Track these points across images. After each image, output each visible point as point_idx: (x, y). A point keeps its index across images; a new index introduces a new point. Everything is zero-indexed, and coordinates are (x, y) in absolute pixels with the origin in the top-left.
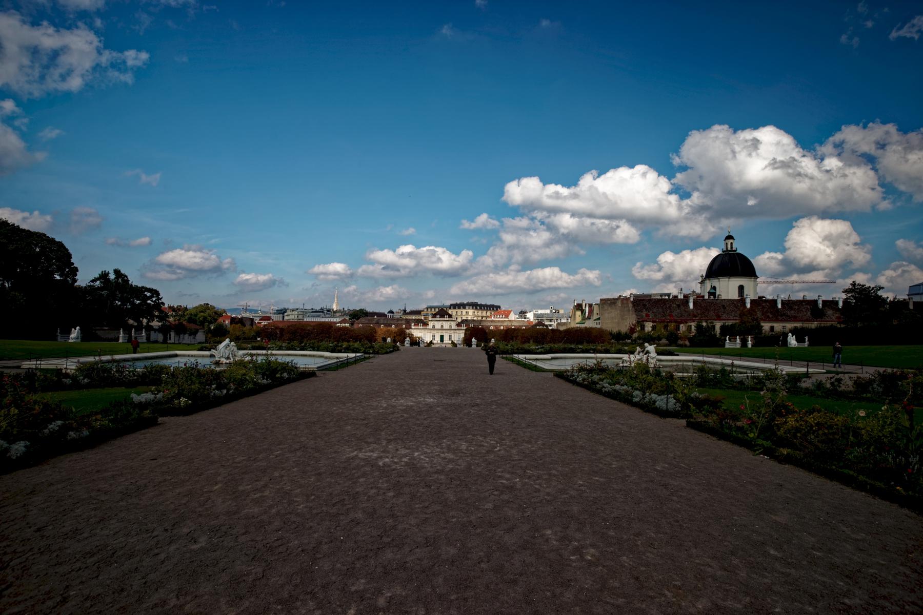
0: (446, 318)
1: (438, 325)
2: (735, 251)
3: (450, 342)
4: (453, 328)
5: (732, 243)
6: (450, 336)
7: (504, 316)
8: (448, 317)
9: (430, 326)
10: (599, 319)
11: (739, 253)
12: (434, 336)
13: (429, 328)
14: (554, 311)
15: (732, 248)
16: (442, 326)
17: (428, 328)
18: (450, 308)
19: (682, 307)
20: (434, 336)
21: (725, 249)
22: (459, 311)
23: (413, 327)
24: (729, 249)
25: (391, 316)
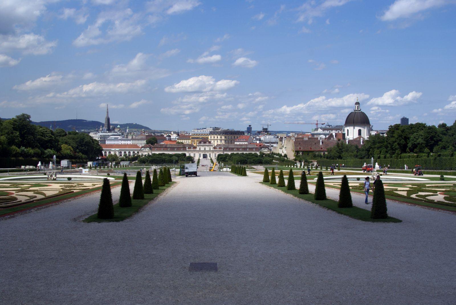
0: (207, 144)
1: (202, 149)
2: (360, 110)
3: (210, 158)
4: (212, 149)
5: (358, 106)
6: (210, 155)
7: (245, 140)
8: (209, 143)
9: (198, 149)
10: (285, 148)
11: (361, 112)
12: (200, 155)
13: (197, 150)
14: (276, 137)
15: (358, 109)
16: (205, 149)
17: (196, 150)
18: (210, 134)
19: (317, 144)
20: (200, 155)
21: (355, 110)
22: (216, 136)
23: (187, 150)
24: (357, 109)
25: (169, 139)
